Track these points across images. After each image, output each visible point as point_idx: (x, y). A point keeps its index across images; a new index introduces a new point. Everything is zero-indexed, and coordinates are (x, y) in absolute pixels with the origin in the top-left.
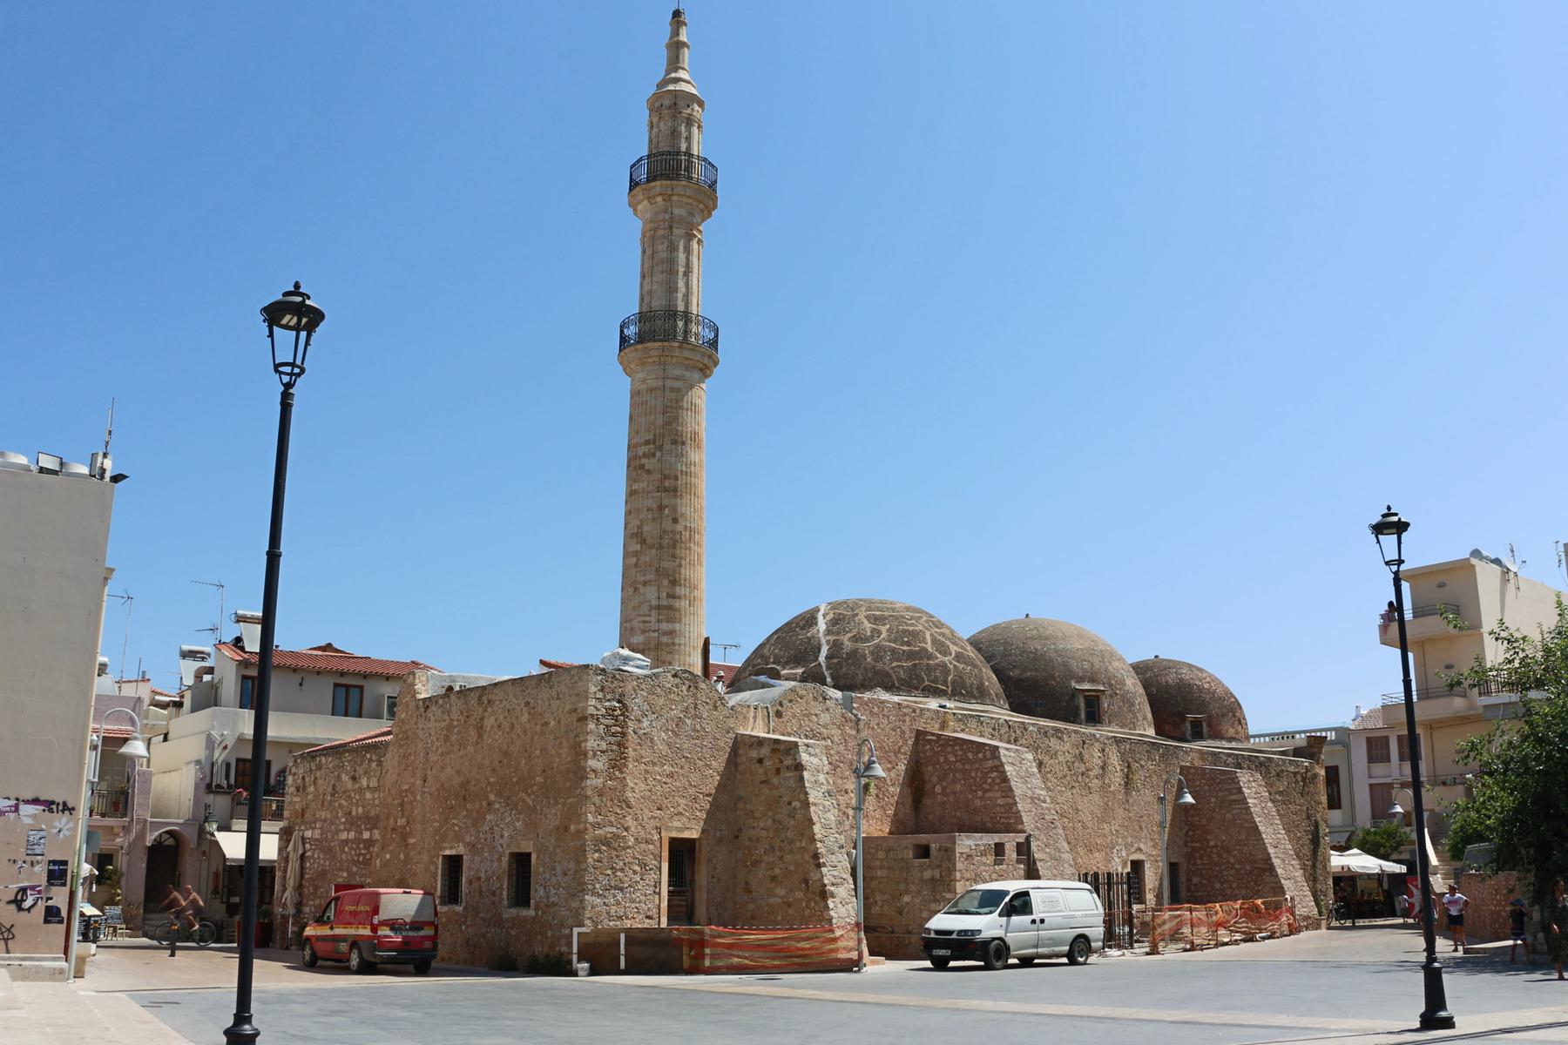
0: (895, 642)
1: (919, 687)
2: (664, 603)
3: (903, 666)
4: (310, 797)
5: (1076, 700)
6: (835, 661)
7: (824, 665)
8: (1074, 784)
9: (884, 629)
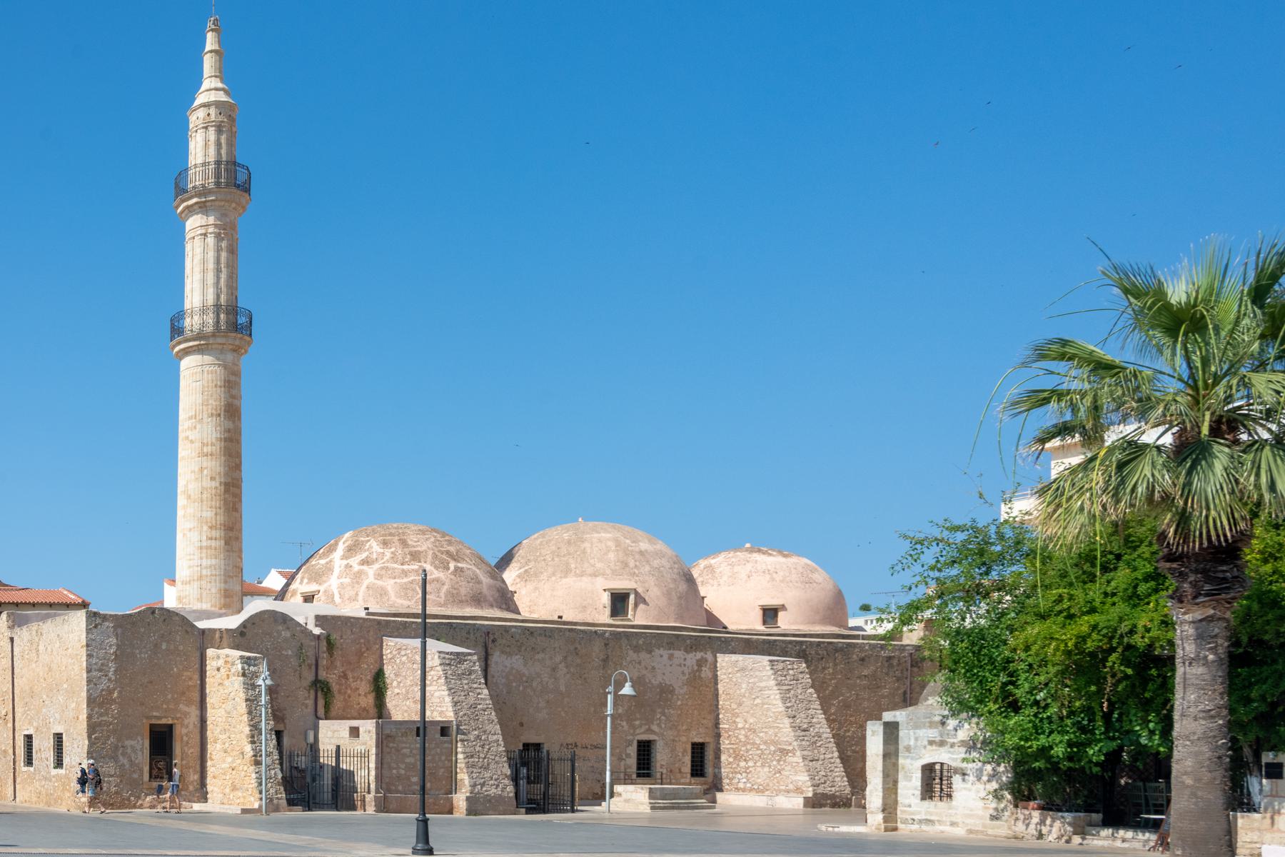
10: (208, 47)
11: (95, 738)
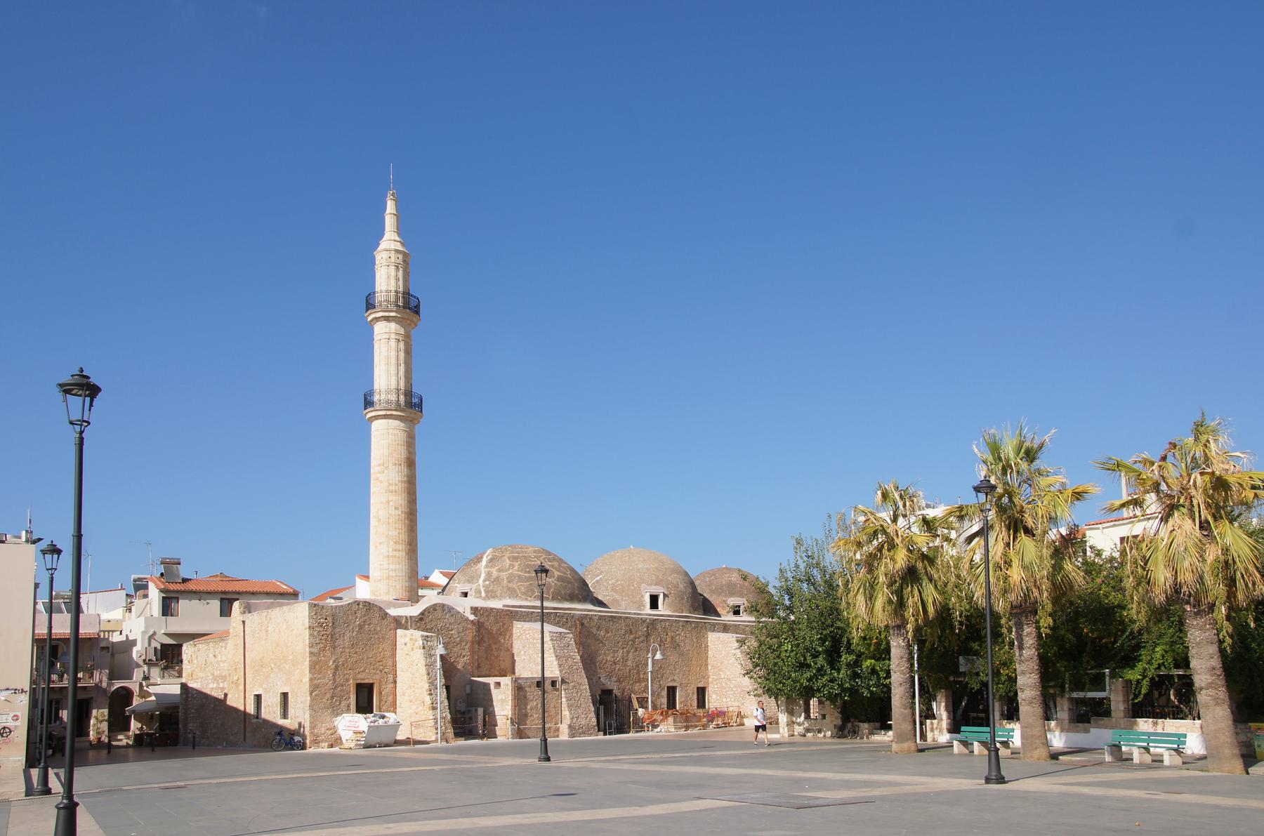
0: (521, 571)
4: (195, 666)
6: (487, 583)
9: (517, 564)
10: (388, 211)
11: (316, 695)
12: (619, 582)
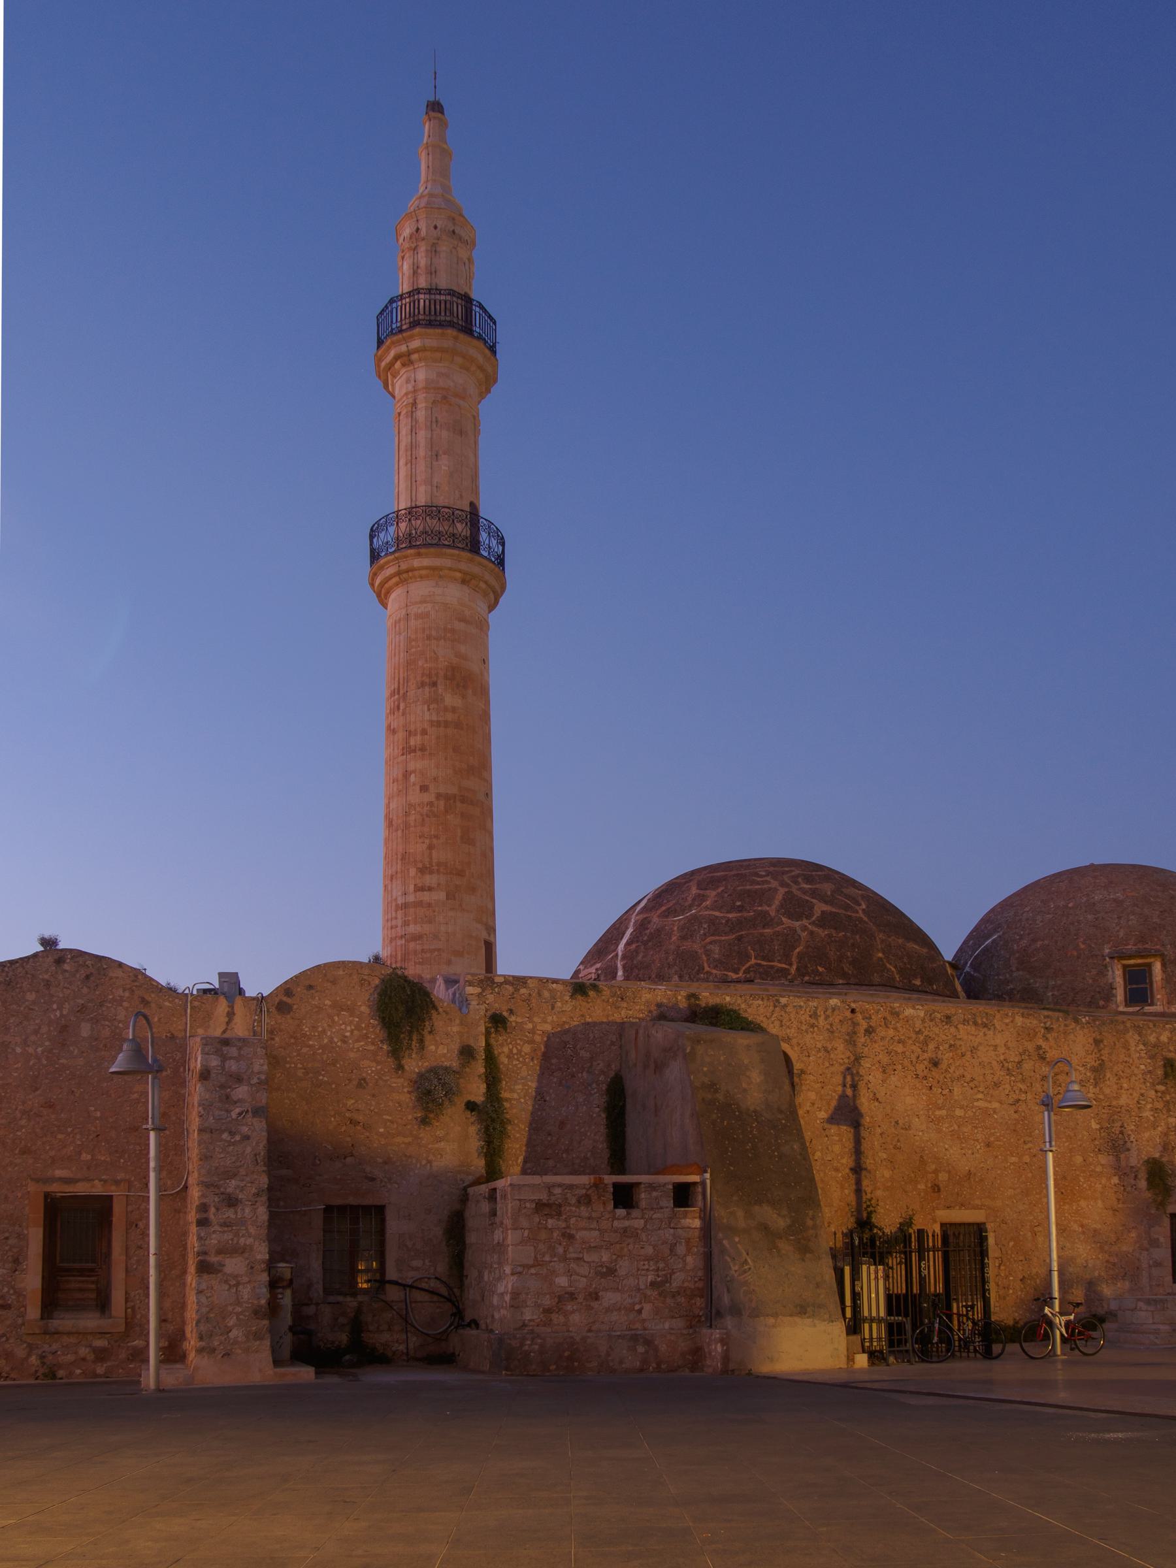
1: (739, 969)
2: (411, 898)
3: (720, 941)
5: (1110, 973)
7: (620, 954)
8: (1023, 1097)
12: (1039, 944)
